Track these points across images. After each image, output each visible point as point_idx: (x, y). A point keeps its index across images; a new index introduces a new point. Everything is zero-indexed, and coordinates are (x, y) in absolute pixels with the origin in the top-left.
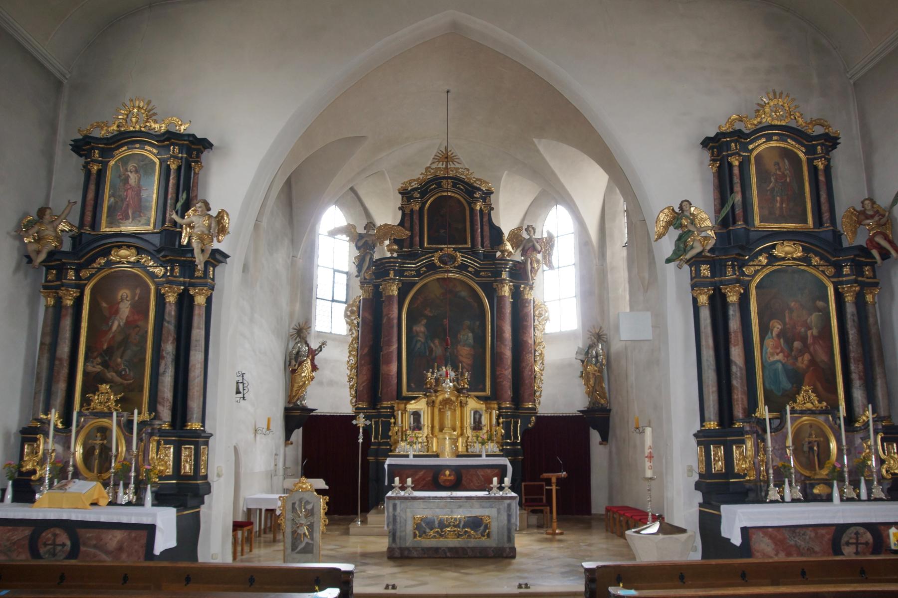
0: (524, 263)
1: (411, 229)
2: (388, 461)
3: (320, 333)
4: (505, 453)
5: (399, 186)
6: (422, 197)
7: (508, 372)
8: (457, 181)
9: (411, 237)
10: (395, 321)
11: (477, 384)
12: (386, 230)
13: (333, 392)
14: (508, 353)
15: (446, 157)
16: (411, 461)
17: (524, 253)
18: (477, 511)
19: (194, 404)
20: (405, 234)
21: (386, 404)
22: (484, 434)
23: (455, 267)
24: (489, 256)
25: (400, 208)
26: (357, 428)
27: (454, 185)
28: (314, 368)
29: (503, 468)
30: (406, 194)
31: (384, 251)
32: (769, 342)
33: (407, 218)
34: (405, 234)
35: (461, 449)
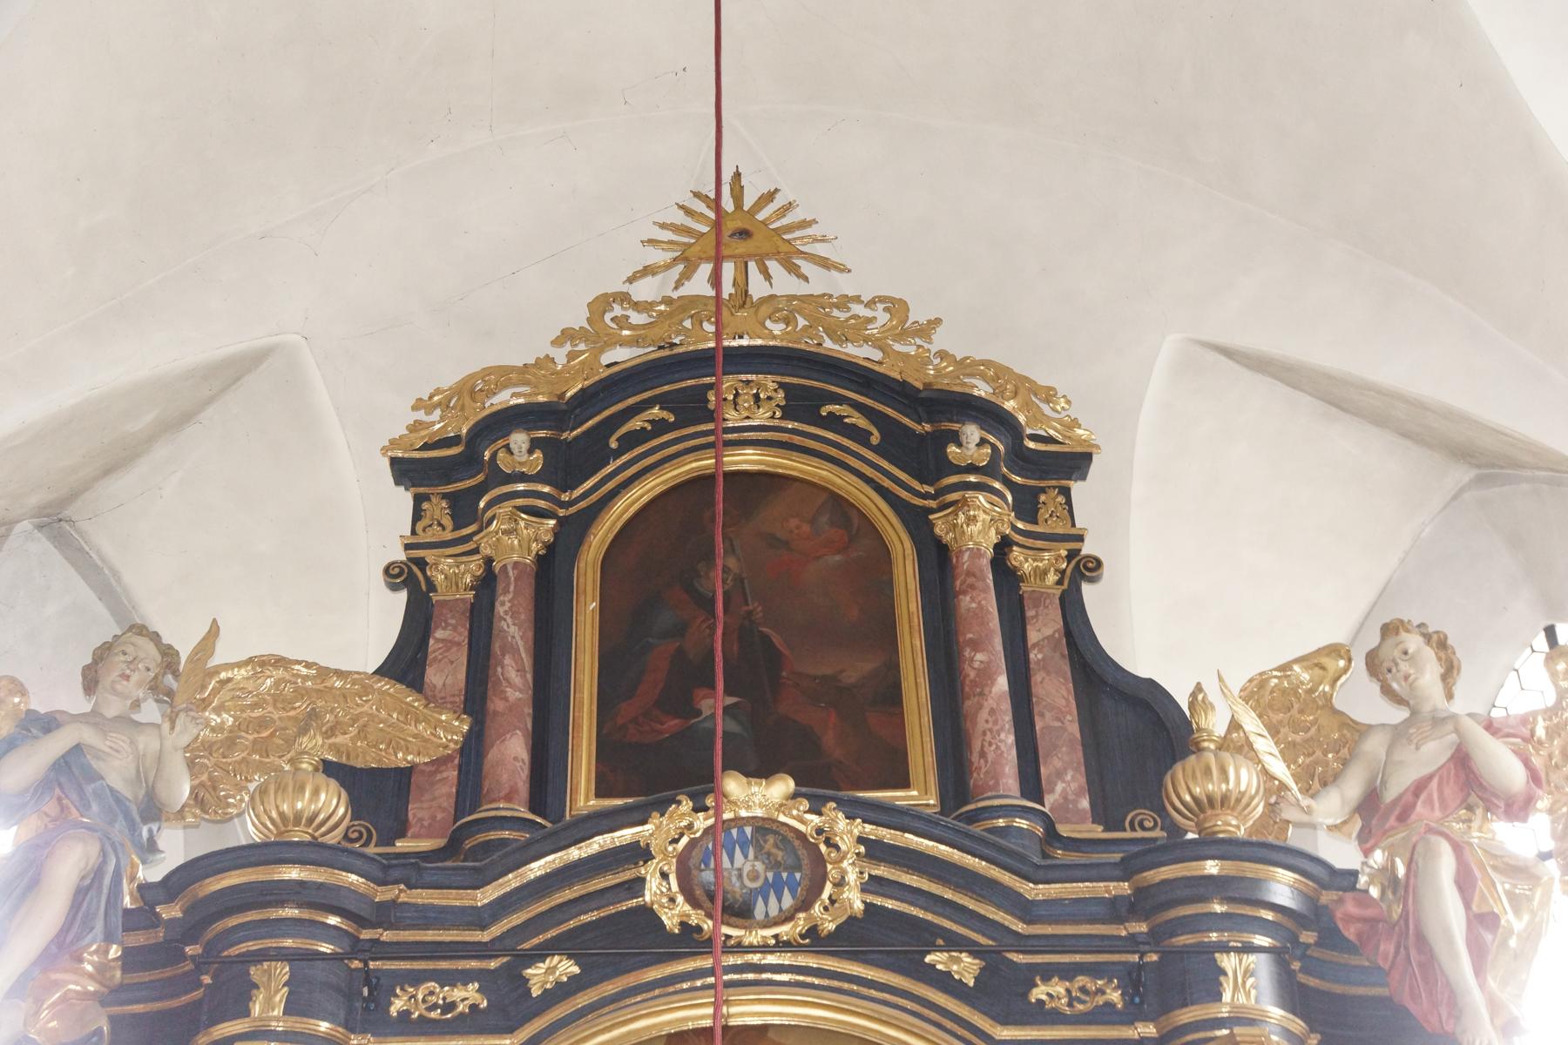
1: (476, 698)
5: (395, 418)
6: (566, 465)
8: (813, 381)
9: (473, 751)
23: (814, 940)
25: (396, 576)
27: (800, 405)
30: (445, 471)
34: (428, 733)
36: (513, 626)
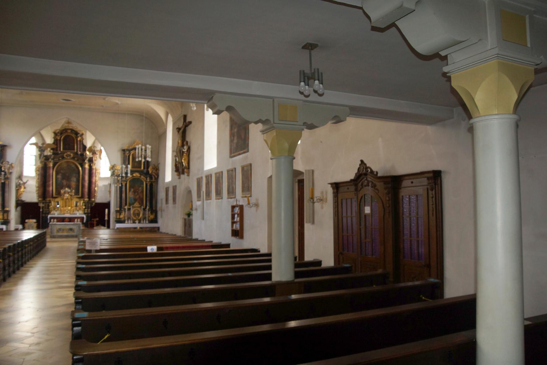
0: (92, 158)
1: (57, 145)
2: (49, 216)
3: (26, 177)
4: (85, 213)
5: (53, 131)
7: (86, 190)
8: (72, 130)
9: (57, 148)
10: (51, 175)
11: (77, 193)
12: (49, 145)
13: (31, 194)
14: (86, 184)
15: (69, 123)
16: (56, 215)
17: (93, 154)
18: (71, 227)
19: (6, 204)
20: (54, 146)
21: (48, 199)
22: (78, 209)
24: (82, 155)
26: (40, 207)
28: (25, 188)
29: (83, 218)
30: (56, 134)
31: (48, 152)
32: (131, 193)
33: (56, 142)
35: (72, 213)
36: (58, 142)
